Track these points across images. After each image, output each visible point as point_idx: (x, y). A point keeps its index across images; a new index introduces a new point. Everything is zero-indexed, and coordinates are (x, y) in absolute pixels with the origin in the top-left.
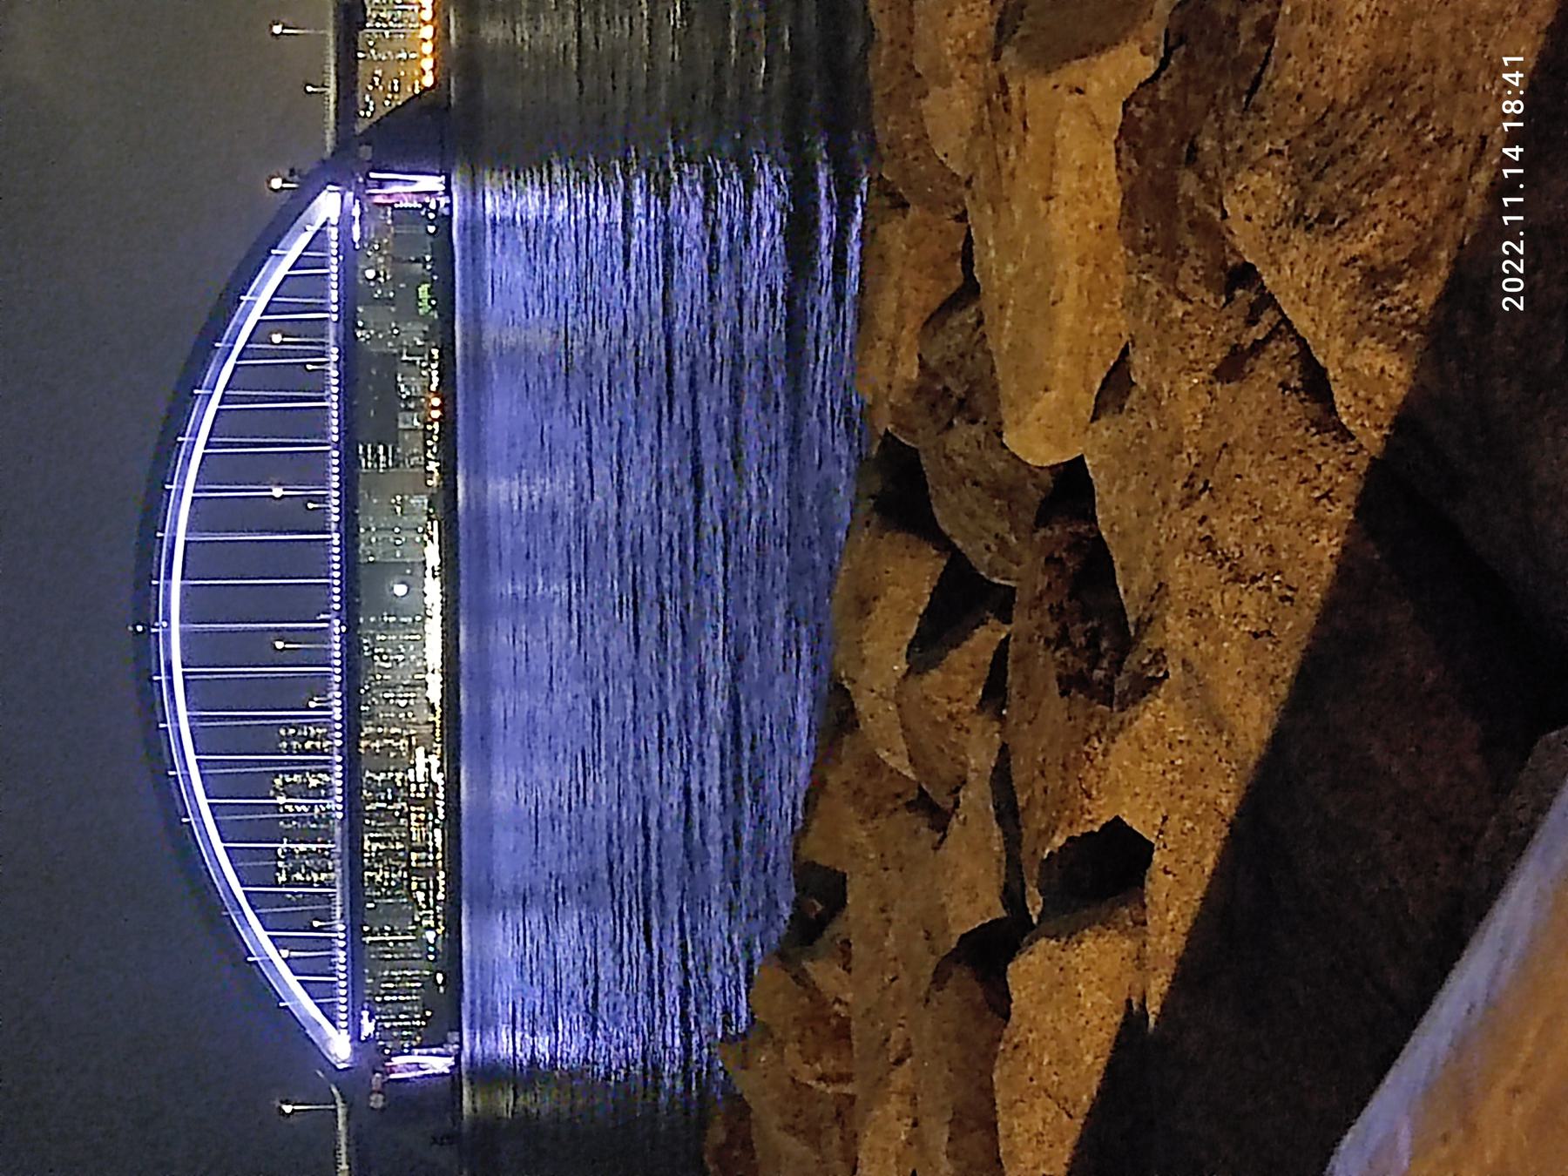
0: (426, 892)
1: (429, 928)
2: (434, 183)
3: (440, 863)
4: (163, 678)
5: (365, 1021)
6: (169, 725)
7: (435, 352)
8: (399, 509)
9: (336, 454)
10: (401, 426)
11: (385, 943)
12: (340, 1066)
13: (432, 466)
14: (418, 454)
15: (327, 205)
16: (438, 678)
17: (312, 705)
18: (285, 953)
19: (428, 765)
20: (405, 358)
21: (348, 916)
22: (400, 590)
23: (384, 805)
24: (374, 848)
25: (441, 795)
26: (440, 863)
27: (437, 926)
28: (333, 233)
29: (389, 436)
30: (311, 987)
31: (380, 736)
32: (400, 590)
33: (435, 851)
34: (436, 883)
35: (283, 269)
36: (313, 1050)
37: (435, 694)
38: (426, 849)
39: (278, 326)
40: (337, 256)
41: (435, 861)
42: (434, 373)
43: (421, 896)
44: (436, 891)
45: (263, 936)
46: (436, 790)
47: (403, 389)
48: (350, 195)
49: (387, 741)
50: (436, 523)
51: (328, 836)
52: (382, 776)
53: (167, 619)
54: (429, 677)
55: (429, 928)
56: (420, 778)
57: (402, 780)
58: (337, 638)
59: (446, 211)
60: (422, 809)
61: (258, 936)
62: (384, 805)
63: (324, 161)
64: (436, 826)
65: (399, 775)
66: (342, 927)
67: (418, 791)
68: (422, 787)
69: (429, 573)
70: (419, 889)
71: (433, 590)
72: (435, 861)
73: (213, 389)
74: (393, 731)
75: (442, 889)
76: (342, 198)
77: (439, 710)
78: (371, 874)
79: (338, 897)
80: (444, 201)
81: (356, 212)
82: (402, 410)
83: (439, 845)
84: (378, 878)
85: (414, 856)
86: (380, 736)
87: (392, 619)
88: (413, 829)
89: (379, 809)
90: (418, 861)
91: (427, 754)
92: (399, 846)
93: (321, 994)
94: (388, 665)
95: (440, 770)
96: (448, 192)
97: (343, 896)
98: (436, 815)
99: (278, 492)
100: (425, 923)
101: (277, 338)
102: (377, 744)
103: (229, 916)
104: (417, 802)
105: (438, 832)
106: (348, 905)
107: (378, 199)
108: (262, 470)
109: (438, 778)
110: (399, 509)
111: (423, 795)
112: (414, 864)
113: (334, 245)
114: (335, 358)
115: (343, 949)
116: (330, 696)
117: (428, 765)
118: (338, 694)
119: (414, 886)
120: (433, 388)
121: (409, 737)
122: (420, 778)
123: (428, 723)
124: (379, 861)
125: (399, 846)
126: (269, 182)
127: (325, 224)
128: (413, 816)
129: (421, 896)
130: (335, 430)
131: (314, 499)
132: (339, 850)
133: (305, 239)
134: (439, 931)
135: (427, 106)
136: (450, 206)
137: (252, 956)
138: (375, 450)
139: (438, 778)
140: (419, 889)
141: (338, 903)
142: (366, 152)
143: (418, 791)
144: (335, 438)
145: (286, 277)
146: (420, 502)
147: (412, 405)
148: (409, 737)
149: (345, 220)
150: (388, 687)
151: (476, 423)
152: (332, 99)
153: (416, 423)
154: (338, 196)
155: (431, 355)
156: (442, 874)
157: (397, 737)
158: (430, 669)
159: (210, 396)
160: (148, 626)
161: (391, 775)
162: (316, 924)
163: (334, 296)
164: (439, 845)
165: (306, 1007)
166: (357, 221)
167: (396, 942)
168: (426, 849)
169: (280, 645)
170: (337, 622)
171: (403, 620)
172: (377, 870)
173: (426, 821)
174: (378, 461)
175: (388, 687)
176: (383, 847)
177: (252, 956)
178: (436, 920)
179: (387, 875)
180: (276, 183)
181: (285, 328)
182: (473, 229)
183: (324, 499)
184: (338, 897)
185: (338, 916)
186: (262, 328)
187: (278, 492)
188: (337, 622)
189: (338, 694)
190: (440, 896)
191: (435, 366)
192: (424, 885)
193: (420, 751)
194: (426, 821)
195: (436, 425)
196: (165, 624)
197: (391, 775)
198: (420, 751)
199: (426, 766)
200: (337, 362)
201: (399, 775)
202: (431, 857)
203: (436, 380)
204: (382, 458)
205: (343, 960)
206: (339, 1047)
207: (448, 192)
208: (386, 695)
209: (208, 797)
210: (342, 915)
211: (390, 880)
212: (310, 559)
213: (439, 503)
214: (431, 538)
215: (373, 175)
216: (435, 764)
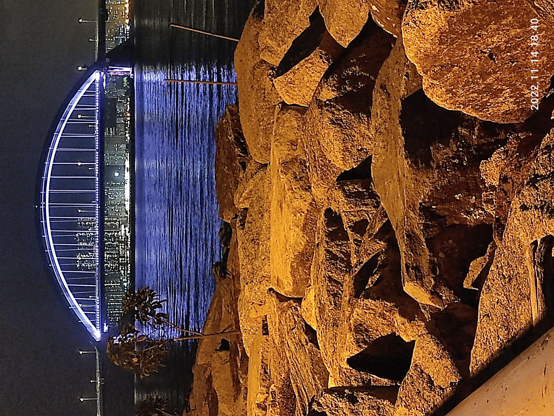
0: (124, 270)
1: (125, 282)
2: (129, 69)
3: (129, 262)
4: (43, 222)
5: (105, 326)
6: (45, 236)
7: (129, 99)
8: (116, 149)
9: (97, 153)
10: (117, 122)
11: (111, 286)
12: (97, 340)
13: (127, 135)
14: (123, 131)
15: (96, 76)
16: (129, 203)
17: (89, 230)
18: (80, 305)
19: (125, 231)
20: (119, 100)
21: (100, 295)
22: (117, 174)
23: (111, 243)
24: (108, 257)
25: (129, 240)
26: (129, 262)
27: (127, 282)
28: (97, 85)
29: (114, 125)
30: (88, 315)
31: (110, 221)
32: (117, 174)
33: (127, 258)
34: (127, 268)
35: (81, 94)
36: (89, 335)
37: (128, 208)
38: (124, 257)
39: (80, 112)
40: (98, 92)
41: (127, 261)
42: (128, 106)
43: (122, 272)
44: (127, 270)
45: (74, 299)
46: (128, 238)
47: (118, 110)
48: (102, 73)
49: (112, 223)
50: (128, 154)
51: (95, 270)
52: (111, 233)
53: (45, 201)
54: (126, 203)
55: (125, 282)
56: (123, 235)
57: (117, 235)
58: (97, 210)
59: (132, 78)
60: (123, 244)
61: (72, 299)
62: (111, 243)
63: (95, 63)
64: (127, 250)
65: (116, 234)
66: (98, 298)
67: (122, 238)
68: (123, 238)
69: (126, 169)
70: (122, 269)
71: (127, 175)
72: (127, 261)
73: (59, 133)
74: (114, 219)
75: (129, 270)
76: (100, 74)
77: (129, 213)
78: (107, 265)
79: (97, 288)
80: (131, 75)
81: (105, 78)
82: (118, 117)
83: (128, 256)
84: (109, 266)
85: (120, 259)
86: (110, 221)
87: (114, 183)
88: (120, 251)
89: (109, 244)
90: (122, 261)
91: (125, 227)
92: (116, 256)
93: (91, 317)
94: (113, 198)
95: (129, 232)
96: (133, 73)
97: (98, 288)
98: (127, 246)
99: (79, 164)
100: (124, 280)
101: (79, 116)
102: (109, 224)
103: (64, 295)
104: (122, 242)
105: (128, 252)
106: (100, 291)
107: (112, 74)
108: (74, 157)
109: (128, 234)
110: (116, 149)
111: (123, 240)
112: (120, 262)
113: (98, 88)
114: (97, 123)
115: (99, 305)
116: (95, 227)
117: (125, 231)
118: (98, 227)
119: (120, 269)
120: (128, 110)
121: (119, 221)
122: (123, 235)
123: (125, 217)
124: (109, 260)
125: (116, 256)
126: (78, 68)
127: (94, 82)
128: (120, 247)
129: (122, 272)
130: (97, 146)
131: (91, 166)
132: (97, 274)
133: (88, 85)
134: (128, 283)
135: (127, 45)
136: (134, 76)
137: (71, 307)
138: (109, 130)
139: (128, 234)
140: (122, 269)
141: (97, 291)
142: (108, 60)
143: (122, 238)
144: (97, 200)
145: (82, 96)
146: (123, 146)
147: (121, 115)
148: (119, 221)
149: (101, 80)
150: (112, 205)
151: (142, 144)
152: (97, 43)
153: (122, 121)
154: (99, 73)
155: (127, 100)
156: (129, 265)
157: (115, 221)
158: (126, 200)
159: (58, 135)
160: (39, 207)
161: (113, 233)
162: (90, 297)
163: (97, 104)
164: (128, 256)
165: (86, 321)
166: (105, 81)
167: (114, 286)
168: (124, 257)
169: (80, 211)
170: (97, 205)
171: (118, 184)
172: (109, 263)
173: (124, 248)
174: (110, 133)
175: (112, 205)
176: (110, 256)
177: (71, 307)
178: (127, 280)
179: (112, 265)
180: (80, 68)
181: (83, 113)
182: (141, 83)
183: (94, 166)
184: (97, 288)
185: (97, 295)
186: (75, 113)
187: (79, 164)
188: (97, 205)
189: (98, 227)
190: (129, 272)
191: (128, 103)
192: (123, 268)
193: (123, 226)
194: (124, 248)
195: (129, 122)
196: (44, 203)
197: (113, 233)
198: (123, 226)
199: (124, 231)
200: (98, 125)
201: (116, 234)
202: (126, 260)
203: (129, 108)
204: (111, 132)
205: (98, 308)
206: (97, 334)
207: (133, 73)
208: (112, 208)
209: (57, 256)
210: (98, 294)
211: (113, 266)
212: (90, 184)
213: (129, 147)
214: (127, 158)
215: (110, 67)
216: (128, 230)
